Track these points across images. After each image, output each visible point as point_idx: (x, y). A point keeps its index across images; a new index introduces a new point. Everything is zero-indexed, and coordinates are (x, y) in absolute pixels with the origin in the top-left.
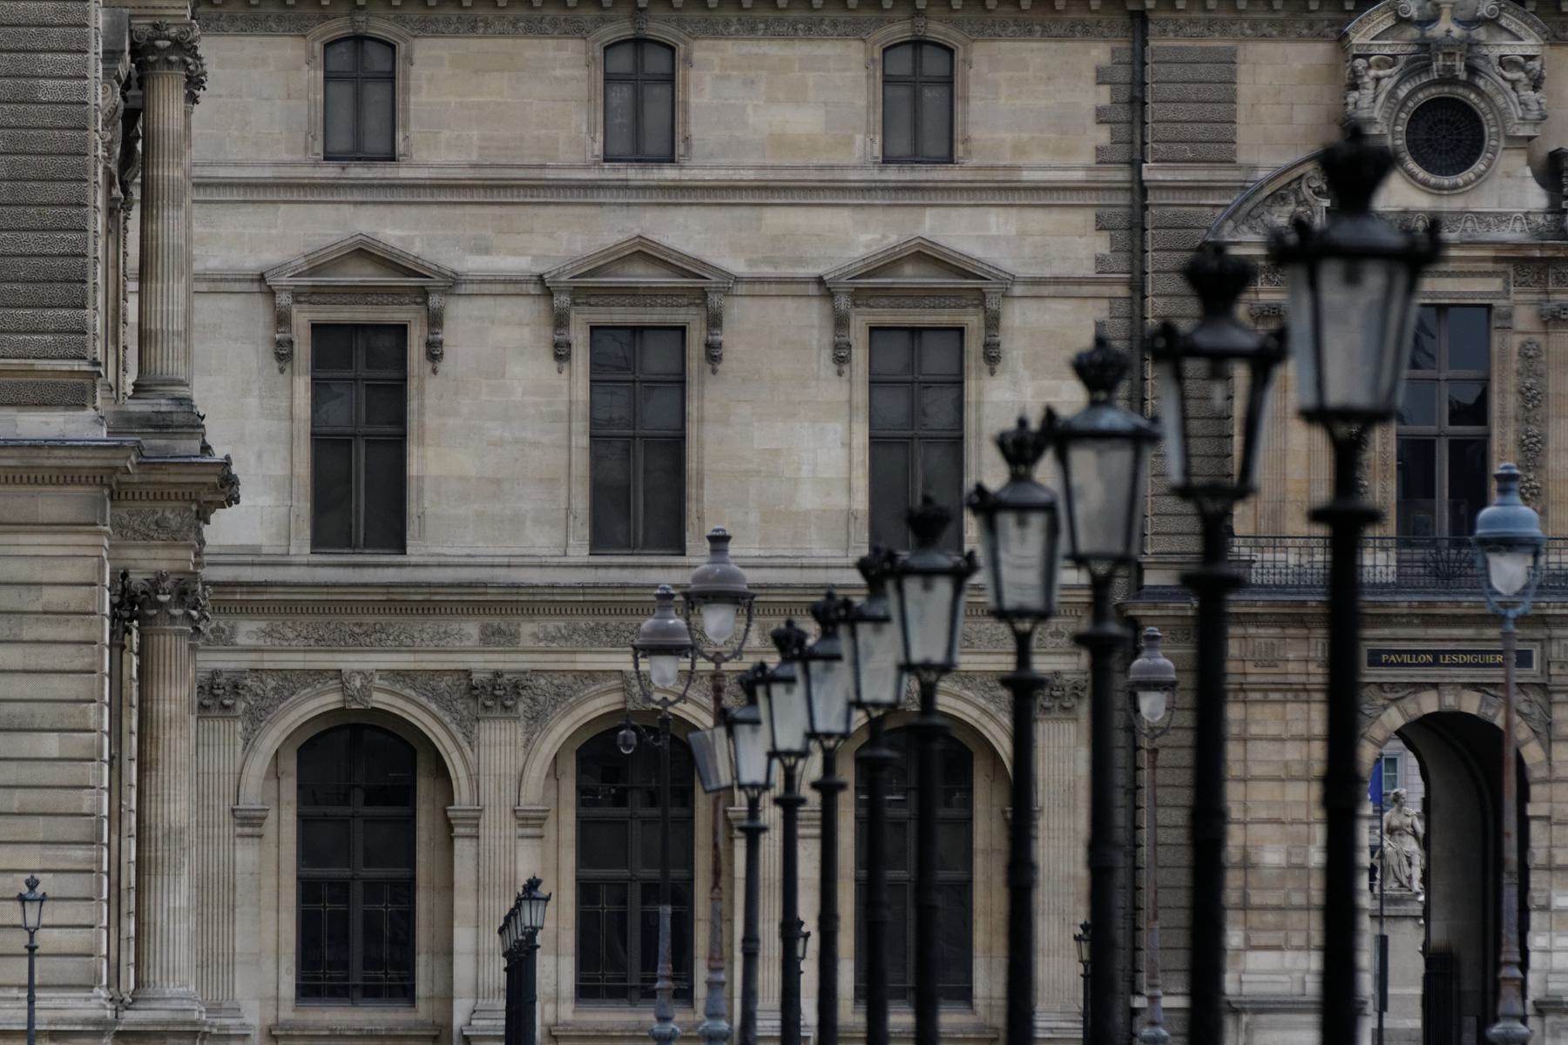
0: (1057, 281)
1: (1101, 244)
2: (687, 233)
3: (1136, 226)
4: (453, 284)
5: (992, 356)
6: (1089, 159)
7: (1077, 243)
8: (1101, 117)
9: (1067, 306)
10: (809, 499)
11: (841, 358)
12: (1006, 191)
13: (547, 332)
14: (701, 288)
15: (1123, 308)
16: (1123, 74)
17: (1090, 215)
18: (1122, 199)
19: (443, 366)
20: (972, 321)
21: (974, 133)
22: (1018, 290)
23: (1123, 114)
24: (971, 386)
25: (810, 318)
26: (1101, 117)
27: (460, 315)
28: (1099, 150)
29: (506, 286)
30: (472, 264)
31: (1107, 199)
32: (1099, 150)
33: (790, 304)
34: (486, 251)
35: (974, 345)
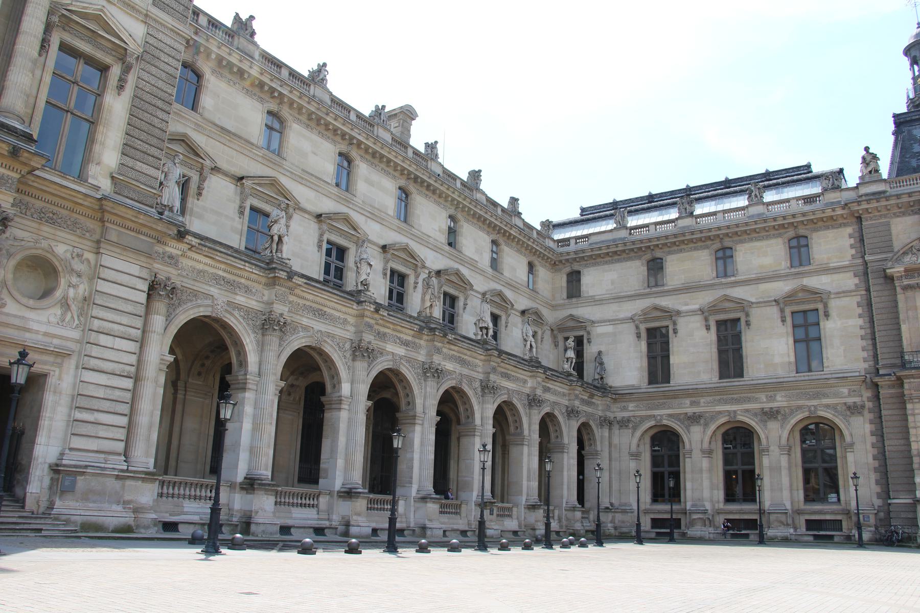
0: (844, 292)
1: (856, 281)
2: (738, 293)
3: (866, 274)
4: (678, 313)
5: (827, 315)
6: (850, 258)
7: (849, 281)
8: (852, 246)
9: (848, 299)
10: (777, 360)
11: (783, 321)
12: (827, 270)
13: (704, 323)
14: (743, 306)
15: (865, 297)
16: (857, 235)
17: (852, 274)
18: (861, 268)
19: (679, 334)
20: (820, 306)
21: (816, 257)
22: (832, 296)
23: (858, 245)
24: (821, 324)
25: (774, 311)
26: (852, 246)
27: (682, 322)
28: (852, 255)
29: (693, 313)
30: (684, 308)
31: (856, 268)
32: (852, 255)
33: (768, 308)
34: (687, 305)
35: (821, 313)
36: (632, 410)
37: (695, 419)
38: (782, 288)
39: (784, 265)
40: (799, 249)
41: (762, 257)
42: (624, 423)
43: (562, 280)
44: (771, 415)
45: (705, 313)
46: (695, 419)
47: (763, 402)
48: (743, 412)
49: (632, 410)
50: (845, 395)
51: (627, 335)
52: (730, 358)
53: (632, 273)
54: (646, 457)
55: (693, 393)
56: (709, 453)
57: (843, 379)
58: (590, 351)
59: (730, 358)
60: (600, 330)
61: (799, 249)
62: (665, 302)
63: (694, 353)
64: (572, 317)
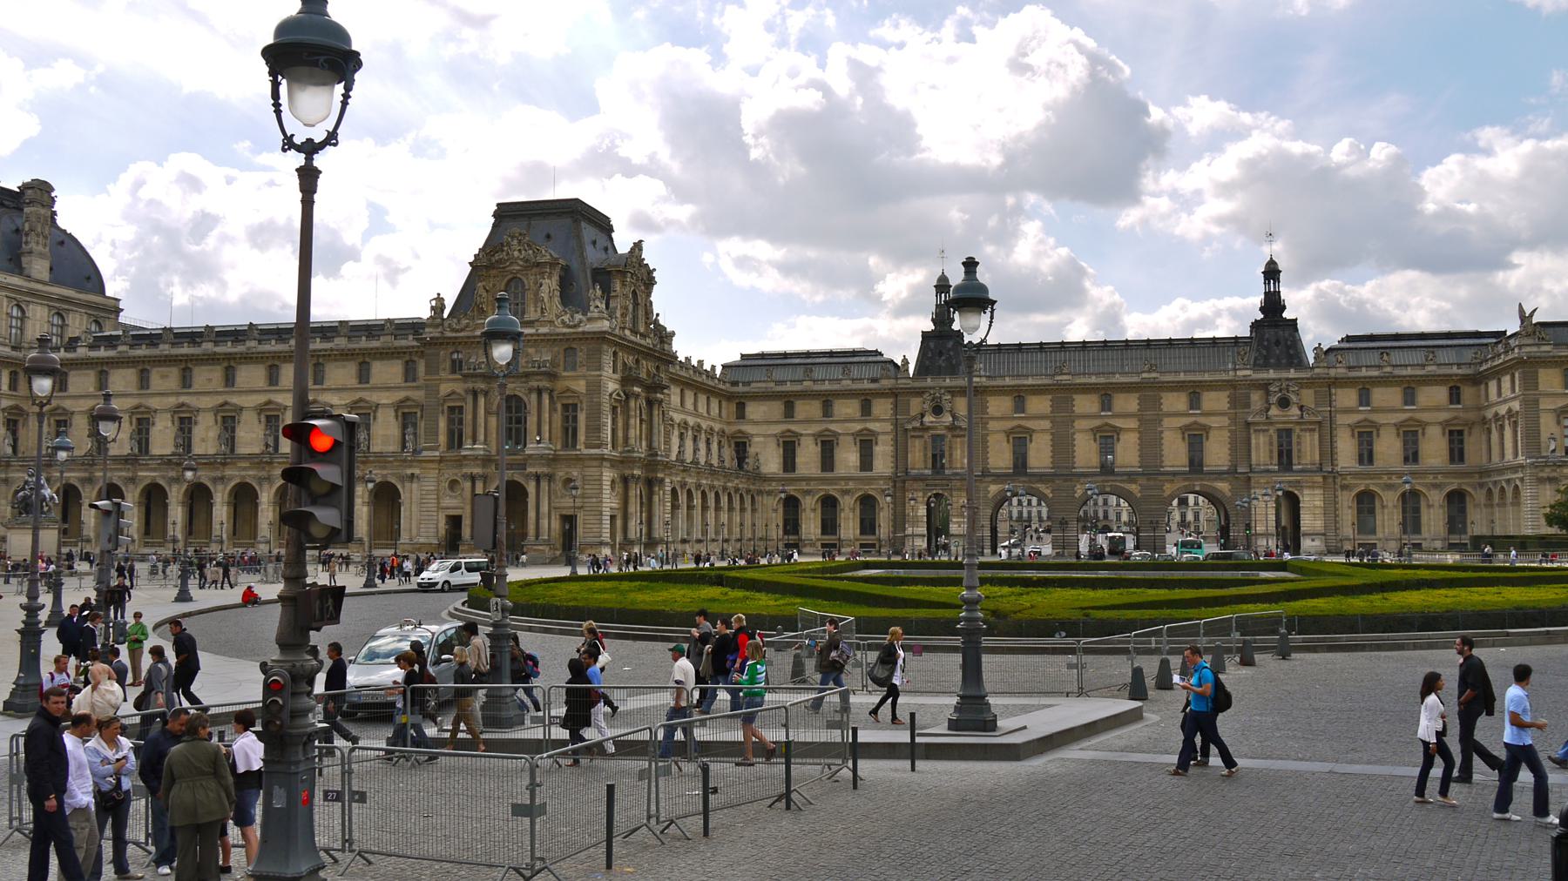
2: (833, 427)
7: (889, 427)
12: (878, 420)
14: (836, 434)
36: (774, 486)
37: (808, 492)
38: (858, 427)
39: (858, 414)
40: (866, 410)
41: (847, 409)
42: (769, 493)
43: (733, 407)
44: (846, 492)
45: (816, 436)
46: (808, 492)
47: (842, 486)
48: (832, 490)
49: (774, 486)
50: (882, 485)
51: (772, 444)
52: (828, 462)
53: (777, 408)
54: (781, 510)
55: (808, 480)
56: (814, 510)
57: (881, 478)
58: (752, 450)
59: (828, 462)
60: (756, 439)
61: (866, 410)
62: (793, 428)
63: (808, 457)
64: (740, 431)
